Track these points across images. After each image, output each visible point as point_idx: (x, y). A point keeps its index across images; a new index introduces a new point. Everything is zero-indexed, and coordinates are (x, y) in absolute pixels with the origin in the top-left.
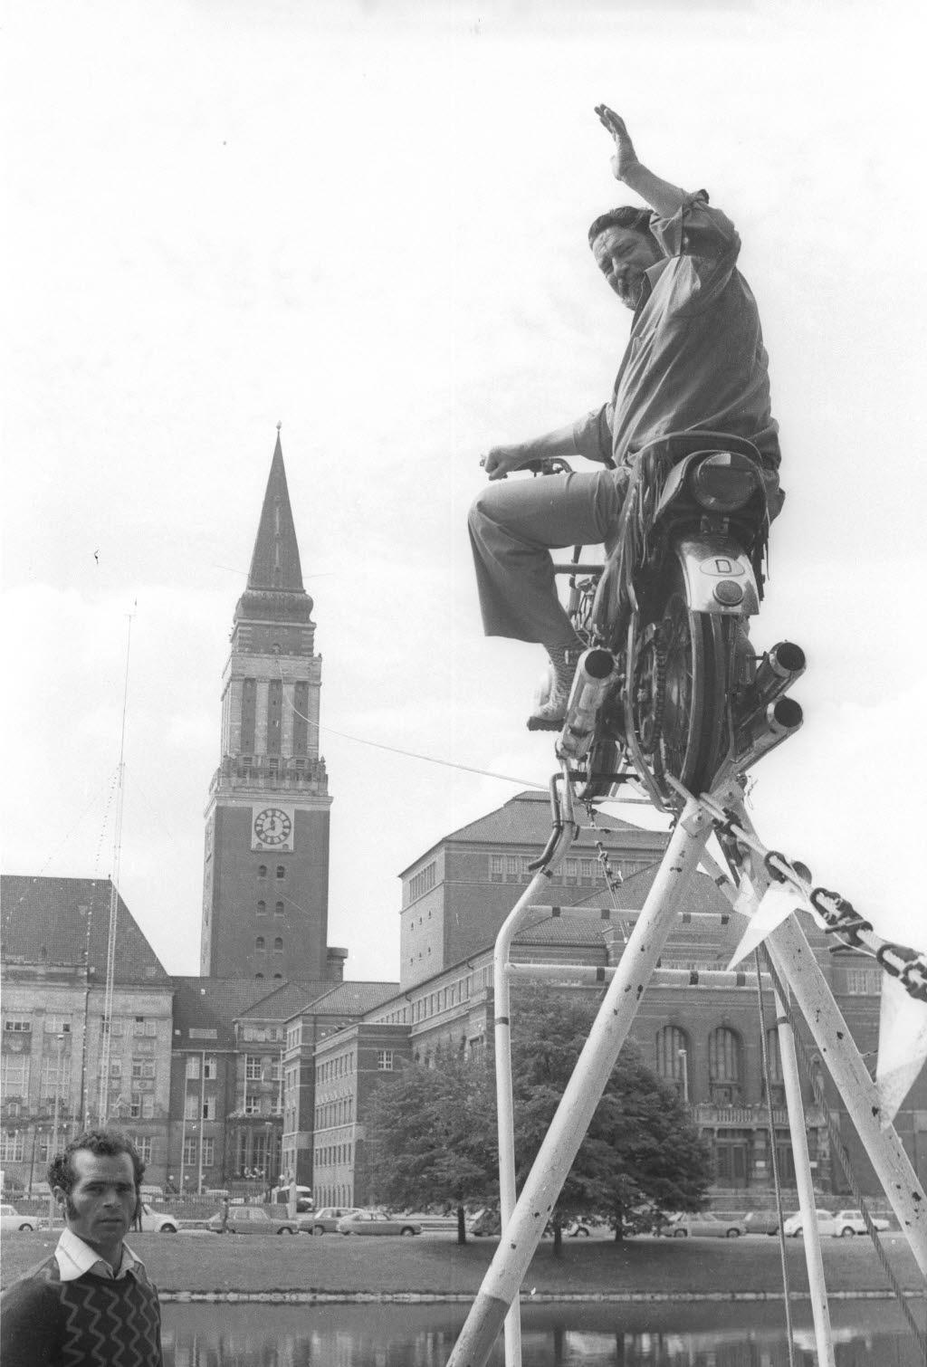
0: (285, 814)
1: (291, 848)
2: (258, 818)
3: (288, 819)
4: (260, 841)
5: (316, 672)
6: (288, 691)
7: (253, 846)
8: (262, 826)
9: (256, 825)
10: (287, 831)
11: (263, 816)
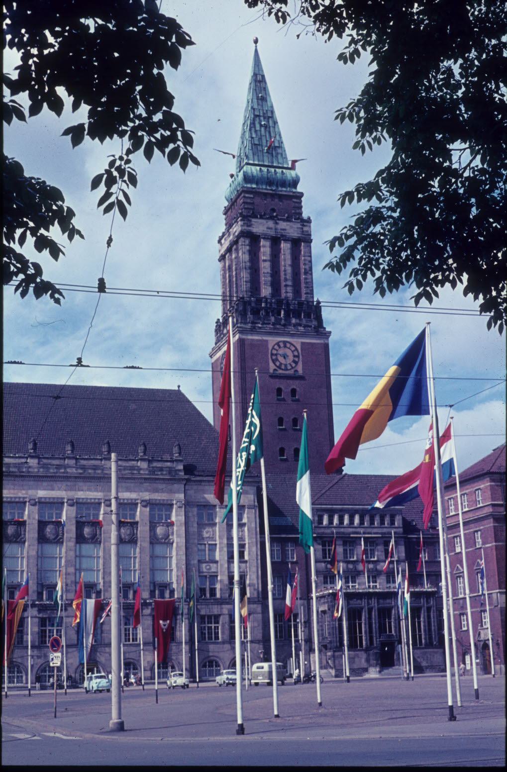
0: (294, 346)
2: (273, 348)
3: (296, 349)
4: (276, 368)
5: (307, 231)
6: (285, 246)
9: (272, 354)
10: (296, 359)
11: (276, 347)
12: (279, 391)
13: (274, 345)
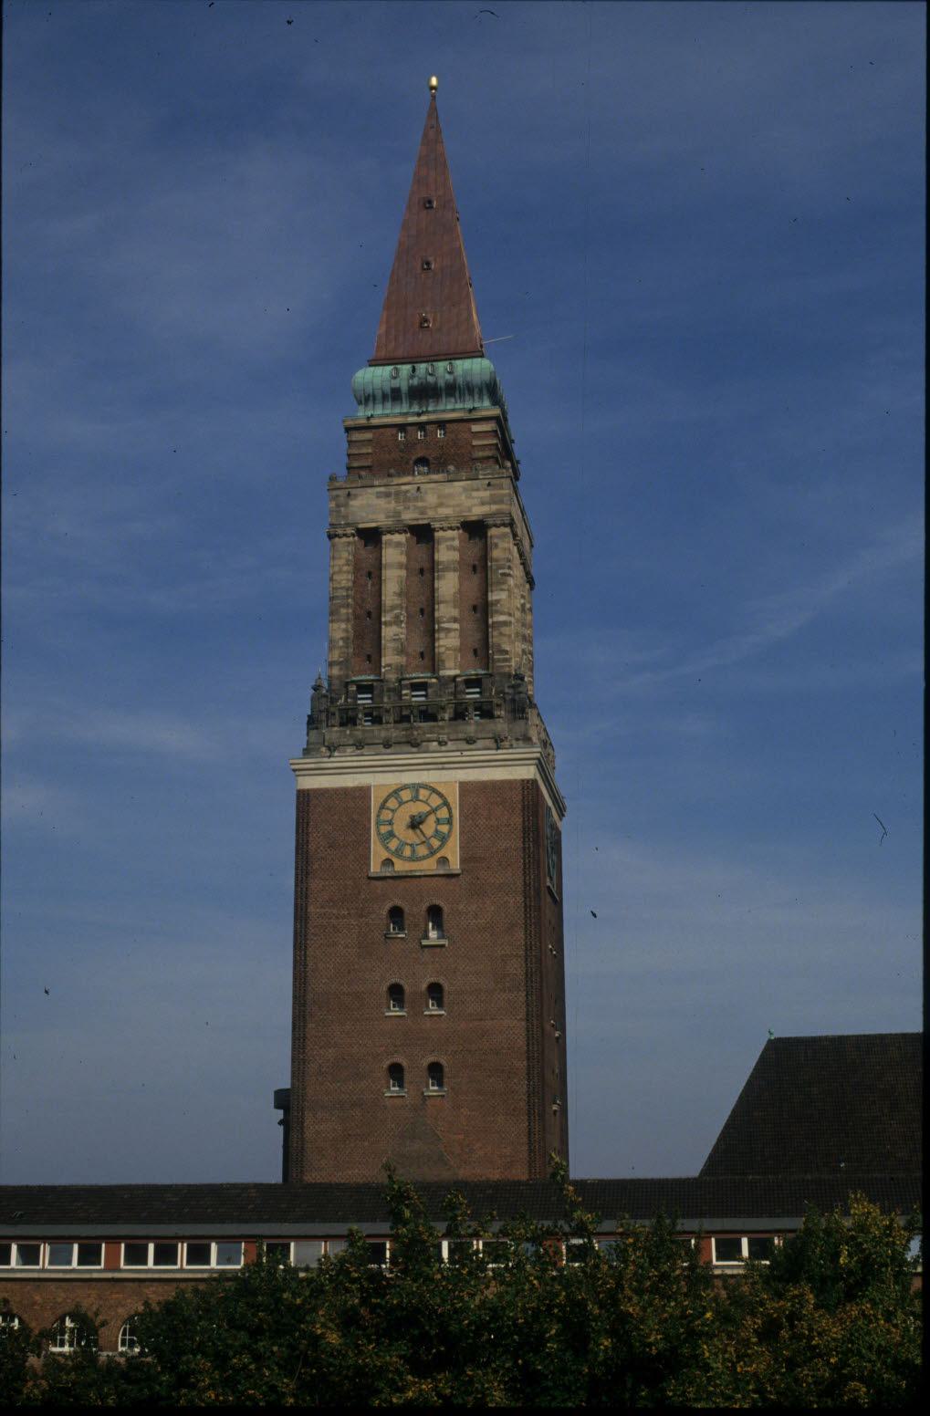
1: (455, 865)
2: (383, 807)
3: (446, 804)
7: (375, 868)
8: (390, 823)
9: (378, 823)
10: (444, 829)
12: (396, 914)
13: (386, 801)
